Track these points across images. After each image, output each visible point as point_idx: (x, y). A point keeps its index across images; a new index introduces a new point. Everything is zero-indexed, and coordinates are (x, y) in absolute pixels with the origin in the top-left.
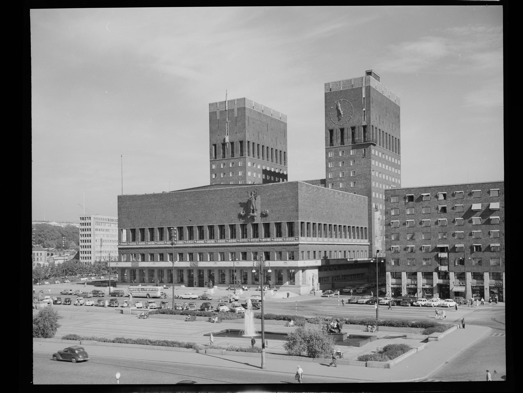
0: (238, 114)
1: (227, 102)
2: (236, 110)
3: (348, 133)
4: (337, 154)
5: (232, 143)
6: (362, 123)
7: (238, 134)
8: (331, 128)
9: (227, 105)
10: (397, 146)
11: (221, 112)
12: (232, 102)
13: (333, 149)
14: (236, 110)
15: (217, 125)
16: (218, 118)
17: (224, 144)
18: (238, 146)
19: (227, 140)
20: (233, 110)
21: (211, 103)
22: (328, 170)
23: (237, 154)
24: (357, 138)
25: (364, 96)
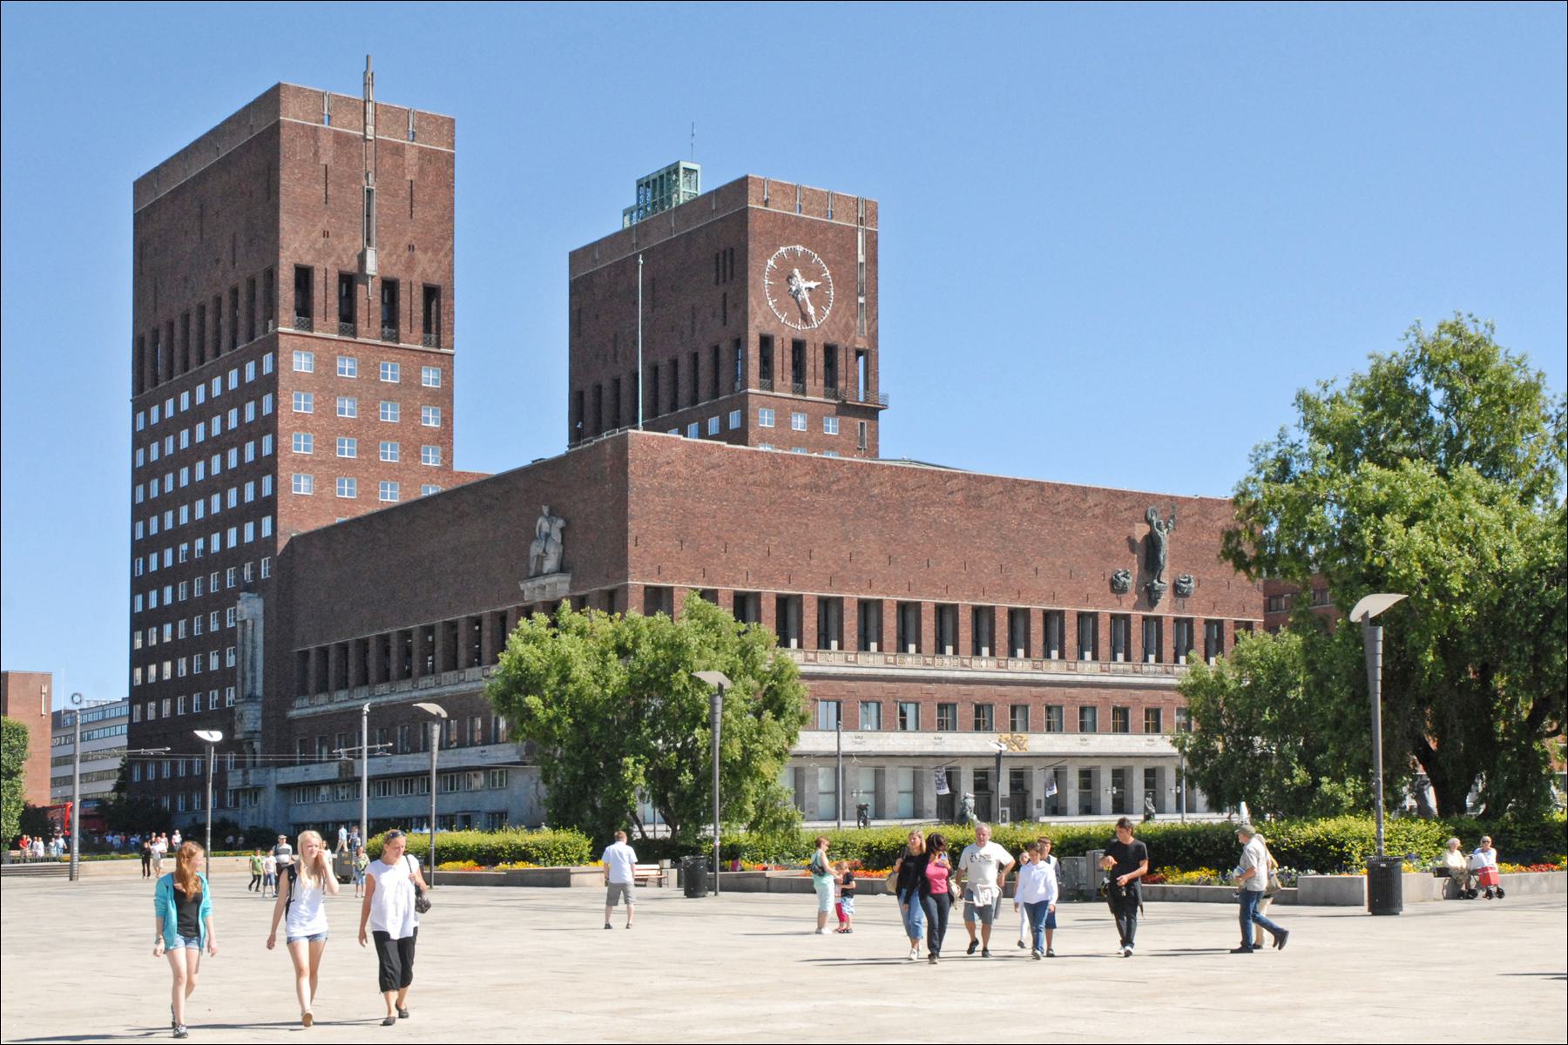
0: (421, 167)
1: (370, 107)
2: (411, 157)
3: (815, 360)
5: (390, 287)
6: (855, 341)
7: (418, 253)
8: (768, 330)
9: (370, 118)
11: (341, 140)
13: (776, 402)
14: (411, 157)
15: (320, 188)
16: (326, 159)
17: (349, 282)
18: (411, 304)
24: (841, 384)
25: (861, 259)
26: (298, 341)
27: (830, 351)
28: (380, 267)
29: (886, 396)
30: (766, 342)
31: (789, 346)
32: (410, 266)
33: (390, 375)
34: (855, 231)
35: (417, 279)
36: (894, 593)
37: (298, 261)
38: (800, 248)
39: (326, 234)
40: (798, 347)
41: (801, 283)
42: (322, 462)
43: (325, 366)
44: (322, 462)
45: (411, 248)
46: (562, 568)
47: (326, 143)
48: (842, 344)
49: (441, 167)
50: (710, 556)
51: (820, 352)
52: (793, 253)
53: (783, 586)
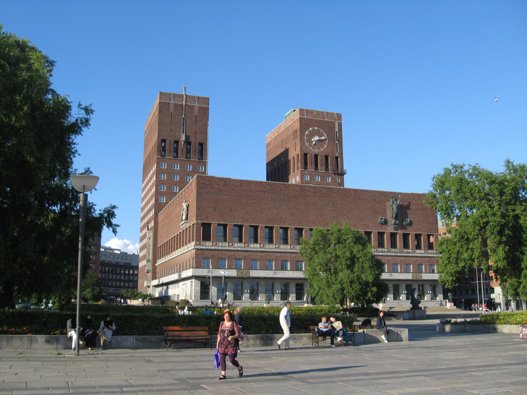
0: (199, 112)
2: (196, 109)
8: (306, 152)
11: (176, 105)
18: (194, 147)
20: (193, 107)
21: (164, 91)
23: (194, 158)
26: (162, 160)
27: (327, 157)
29: (346, 170)
30: (305, 155)
31: (313, 156)
32: (195, 138)
33: (190, 168)
34: (334, 122)
35: (198, 142)
36: (294, 225)
37: (162, 138)
38: (316, 128)
39: (171, 131)
40: (316, 156)
42: (168, 193)
43: (170, 166)
44: (168, 193)
45: (196, 133)
46: (187, 218)
49: (205, 112)
50: (226, 213)
51: (324, 158)
52: (314, 130)
53: (252, 223)
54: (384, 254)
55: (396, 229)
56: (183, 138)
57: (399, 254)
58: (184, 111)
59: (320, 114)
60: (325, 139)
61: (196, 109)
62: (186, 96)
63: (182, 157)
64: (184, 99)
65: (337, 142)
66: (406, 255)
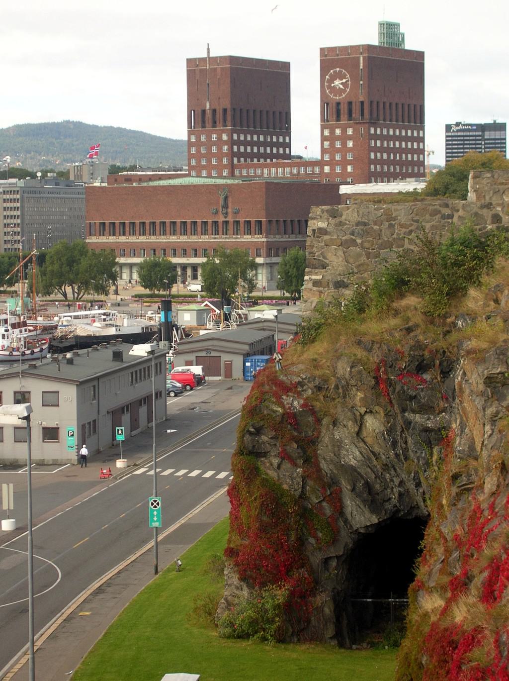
2: (219, 71)
3: (344, 108)
4: (332, 132)
5: (214, 111)
6: (359, 98)
10: (418, 114)
11: (201, 71)
12: (215, 59)
17: (204, 112)
19: (208, 107)
20: (215, 69)
22: (323, 151)
24: (354, 115)
27: (350, 103)
28: (210, 105)
31: (334, 105)
33: (214, 137)
34: (359, 58)
38: (338, 69)
39: (198, 100)
41: (337, 83)
42: (197, 167)
44: (197, 167)
45: (219, 98)
47: (197, 72)
48: (354, 100)
54: (215, 240)
55: (226, 217)
56: (208, 107)
57: (228, 240)
58: (208, 77)
59: (344, 49)
60: (348, 81)
61: (219, 71)
62: (209, 58)
63: (209, 128)
64: (208, 62)
65: (361, 82)
66: (234, 240)
